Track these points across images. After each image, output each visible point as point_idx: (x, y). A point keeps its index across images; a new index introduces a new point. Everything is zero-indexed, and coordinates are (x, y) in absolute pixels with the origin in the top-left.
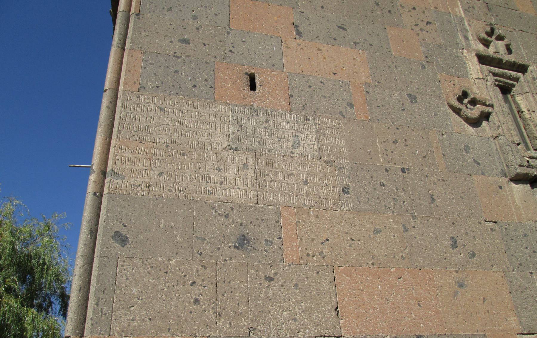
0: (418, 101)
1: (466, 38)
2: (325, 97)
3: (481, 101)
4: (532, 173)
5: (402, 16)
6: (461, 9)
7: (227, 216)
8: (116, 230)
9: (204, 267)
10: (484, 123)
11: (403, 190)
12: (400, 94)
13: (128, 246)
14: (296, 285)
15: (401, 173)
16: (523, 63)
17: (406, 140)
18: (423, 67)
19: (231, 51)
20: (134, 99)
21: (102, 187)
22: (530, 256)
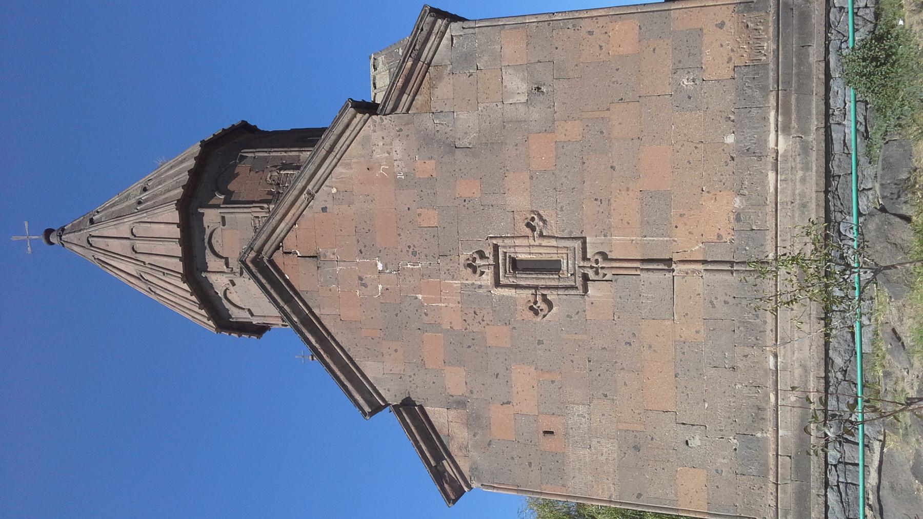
0: (541, 339)
1: (480, 287)
2: (550, 395)
7: (625, 453)
8: (635, 497)
9: (649, 465)
10: (549, 297)
11: (601, 364)
13: (642, 493)
14: (654, 428)
15: (591, 363)
18: (514, 328)
19: (531, 442)
20: (570, 489)
21: (617, 502)
22: (633, 299)
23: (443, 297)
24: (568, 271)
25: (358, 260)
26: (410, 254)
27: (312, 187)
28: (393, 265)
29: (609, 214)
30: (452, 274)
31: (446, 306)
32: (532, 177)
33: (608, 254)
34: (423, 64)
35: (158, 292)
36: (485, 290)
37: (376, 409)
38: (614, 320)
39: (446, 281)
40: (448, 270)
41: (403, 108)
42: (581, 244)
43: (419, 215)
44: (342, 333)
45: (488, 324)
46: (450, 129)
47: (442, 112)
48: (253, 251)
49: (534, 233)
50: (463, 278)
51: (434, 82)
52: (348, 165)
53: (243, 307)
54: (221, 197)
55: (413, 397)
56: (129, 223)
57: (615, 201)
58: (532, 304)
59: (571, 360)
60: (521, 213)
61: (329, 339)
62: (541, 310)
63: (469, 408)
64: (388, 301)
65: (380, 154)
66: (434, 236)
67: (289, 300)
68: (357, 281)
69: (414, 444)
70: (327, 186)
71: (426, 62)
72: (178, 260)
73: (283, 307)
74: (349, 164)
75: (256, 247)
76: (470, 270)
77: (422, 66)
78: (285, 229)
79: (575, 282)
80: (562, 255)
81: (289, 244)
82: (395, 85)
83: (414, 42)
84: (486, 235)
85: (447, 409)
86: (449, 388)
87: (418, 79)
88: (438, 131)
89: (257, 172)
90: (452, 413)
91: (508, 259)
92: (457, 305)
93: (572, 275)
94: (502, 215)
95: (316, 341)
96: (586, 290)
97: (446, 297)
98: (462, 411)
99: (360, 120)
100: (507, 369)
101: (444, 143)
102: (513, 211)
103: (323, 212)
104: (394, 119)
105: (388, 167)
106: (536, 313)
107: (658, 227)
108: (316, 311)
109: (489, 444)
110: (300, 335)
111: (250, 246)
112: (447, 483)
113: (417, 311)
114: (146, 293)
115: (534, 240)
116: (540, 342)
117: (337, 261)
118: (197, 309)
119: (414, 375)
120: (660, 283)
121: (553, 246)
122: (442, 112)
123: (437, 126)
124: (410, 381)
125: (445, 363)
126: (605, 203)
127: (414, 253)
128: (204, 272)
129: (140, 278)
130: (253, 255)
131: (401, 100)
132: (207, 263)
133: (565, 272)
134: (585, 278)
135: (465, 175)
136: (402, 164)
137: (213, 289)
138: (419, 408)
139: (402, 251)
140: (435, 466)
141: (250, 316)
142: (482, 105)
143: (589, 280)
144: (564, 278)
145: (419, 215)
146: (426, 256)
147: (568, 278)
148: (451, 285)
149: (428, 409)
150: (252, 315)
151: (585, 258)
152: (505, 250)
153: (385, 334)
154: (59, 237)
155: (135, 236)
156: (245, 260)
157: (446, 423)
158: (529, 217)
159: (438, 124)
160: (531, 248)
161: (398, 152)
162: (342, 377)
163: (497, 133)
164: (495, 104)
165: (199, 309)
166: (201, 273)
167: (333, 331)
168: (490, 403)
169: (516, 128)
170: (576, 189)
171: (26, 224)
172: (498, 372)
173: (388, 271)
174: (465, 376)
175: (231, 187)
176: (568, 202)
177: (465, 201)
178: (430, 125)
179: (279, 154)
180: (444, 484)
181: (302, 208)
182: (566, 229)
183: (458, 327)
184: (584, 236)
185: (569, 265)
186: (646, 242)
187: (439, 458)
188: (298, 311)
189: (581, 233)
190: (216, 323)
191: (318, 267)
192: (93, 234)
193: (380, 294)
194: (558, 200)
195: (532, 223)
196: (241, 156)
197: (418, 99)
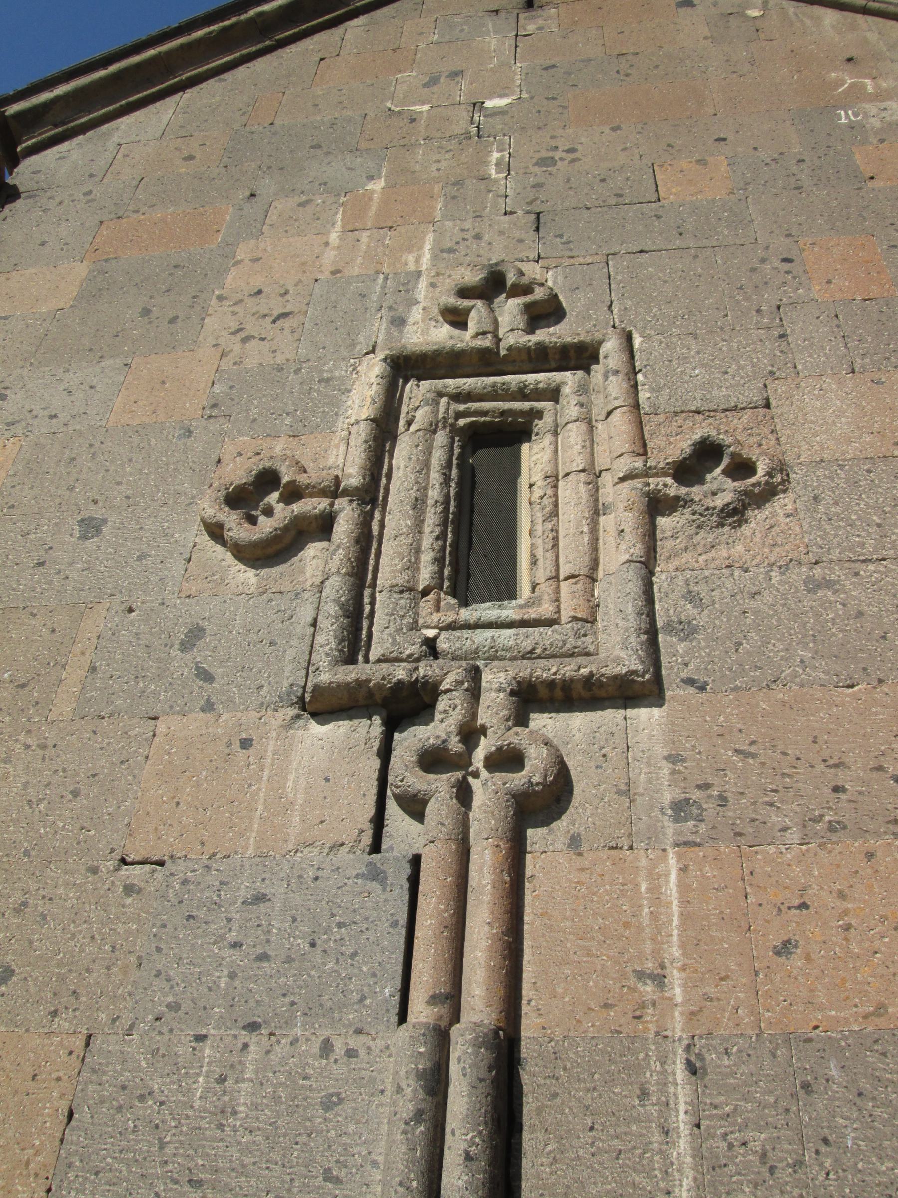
3: (314, 487)
4: (383, 679)
10: (313, 550)
16: (575, 341)
22: (232, 976)
24: (451, 627)
29: (831, 828)
33: (562, 825)
38: (123, 861)
49: (665, 475)
50: (438, 274)
58: (285, 479)
60: (767, 431)
84: (639, 325)
91: (526, 405)
94: (740, 368)
102: (768, 406)
107: (784, 1174)
115: (622, 479)
120: (328, 1176)
143: (392, 725)
152: (566, 390)
158: (752, 453)
184: (668, 694)
185: (489, 633)
186: (651, 1078)
189: (690, 682)
191: (497, 12)
194: (871, 567)
195: (718, 470)
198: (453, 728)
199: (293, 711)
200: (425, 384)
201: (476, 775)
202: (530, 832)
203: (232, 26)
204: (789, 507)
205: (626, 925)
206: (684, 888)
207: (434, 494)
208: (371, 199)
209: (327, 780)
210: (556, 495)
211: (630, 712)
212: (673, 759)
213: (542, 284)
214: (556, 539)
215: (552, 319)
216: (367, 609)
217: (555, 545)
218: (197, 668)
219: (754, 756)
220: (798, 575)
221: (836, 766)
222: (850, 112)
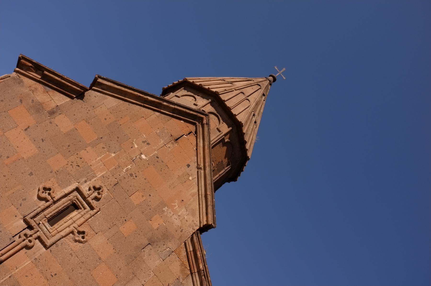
0: (32, 176)
1: (86, 182)
2: (4, 149)
5: (72, 156)
6: (101, 174)
10: (44, 202)
12: (29, 169)
17: (8, 179)
18: (51, 172)
23: (101, 163)
24: (43, 224)
25: (156, 152)
26: (133, 173)
27: (201, 172)
28: (137, 162)
30: (105, 178)
31: (96, 159)
32: (100, 259)
34: (194, 271)
35: (220, 81)
36: (81, 182)
37: (95, 83)
39: (106, 172)
40: (108, 179)
41: (188, 243)
42: (47, 244)
43: (143, 196)
44: (138, 111)
45: (67, 164)
46: (159, 251)
47: (169, 256)
48: (206, 123)
49: (77, 230)
51: (183, 267)
52: (193, 195)
53: (182, 97)
54: (227, 140)
55: (79, 101)
56: (252, 103)
57: (44, 282)
58: (50, 192)
59: (5, 176)
61: (142, 104)
62: (43, 192)
63: (47, 113)
64: (127, 141)
65: (183, 212)
66: (128, 191)
67: (174, 111)
68: (149, 141)
69: (63, 76)
70: (195, 178)
71: (194, 273)
72: (226, 99)
73: (174, 105)
74: (193, 196)
75: (206, 126)
76: (97, 186)
77: (194, 270)
78: (199, 143)
79: (35, 221)
80: (53, 230)
81: (192, 138)
82: (200, 251)
83: (206, 279)
84: (102, 211)
85: (57, 106)
86: (64, 117)
87: (192, 262)
88: (164, 245)
89: (219, 162)
90: (53, 105)
92: (91, 164)
93: (40, 223)
95: (147, 99)
96: (25, 221)
97: (100, 164)
98: (49, 109)
99: (203, 221)
100: (39, 147)
101: (157, 241)
102: (96, 234)
103: (188, 164)
104: (188, 235)
105: (174, 208)
106: (45, 189)
108: (158, 114)
109: (21, 101)
110: (157, 97)
111: (209, 125)
112: (31, 66)
113: (109, 147)
114: (224, 78)
115: (74, 227)
116: (31, 174)
117: (165, 145)
118: (202, 83)
119: (88, 113)
121: (61, 231)
122: (169, 256)
123: (166, 247)
124: (87, 108)
125: (76, 129)
126: (49, 276)
127: (131, 175)
128: (210, 102)
129: (231, 83)
130: (205, 121)
131: (192, 245)
132: (212, 107)
133: (44, 222)
134: (30, 227)
135: (135, 234)
136: (169, 215)
137: (201, 97)
138: (73, 97)
139: (138, 172)
140: (43, 72)
141: (177, 95)
142: (152, 275)
143: (27, 228)
144: (43, 218)
145: (143, 196)
146: (124, 178)
147: (41, 220)
148: (101, 171)
149: (68, 99)
150: (176, 96)
151: (39, 238)
152: (86, 210)
153: (117, 124)
154: (270, 80)
155: (246, 99)
156: (206, 117)
157: (53, 98)
159: (167, 248)
160: (73, 222)
161: (175, 220)
162: (123, 89)
163: (134, 267)
164: (146, 281)
165: (201, 84)
166: (211, 100)
167: (143, 109)
168: (37, 123)
169: (127, 278)
170: (71, 271)
171: (284, 78)
172: (44, 142)
173: (138, 157)
174: (60, 129)
175: (225, 148)
176: (71, 261)
177: (125, 220)
178: (170, 245)
179: (216, 177)
180: (32, 65)
181: (199, 159)
182: (61, 245)
183: (82, 153)
184: (48, 250)
185: (44, 228)
187: (44, 77)
188: (166, 108)
190: (189, 83)
191: (172, 136)
192: (260, 90)
193: (134, 143)
194: (77, 258)
196: (230, 165)
197: (184, 253)
198: (30, 234)
199: (23, 217)
200: (77, 193)
201: (27, 239)
202: (24, 248)
203: (141, 97)
204: (81, 245)
205: (20, 263)
206: (27, 265)
207: (60, 208)
208: (110, 157)
209: (17, 227)
210: (68, 221)
211: (44, 248)
212: (41, 255)
213: (102, 195)
214: (62, 225)
215: (97, 200)
216: (40, 214)
217: (61, 226)
218: (21, 204)
219: (46, 261)
220: (71, 252)
221: (49, 269)
222: (167, 209)
